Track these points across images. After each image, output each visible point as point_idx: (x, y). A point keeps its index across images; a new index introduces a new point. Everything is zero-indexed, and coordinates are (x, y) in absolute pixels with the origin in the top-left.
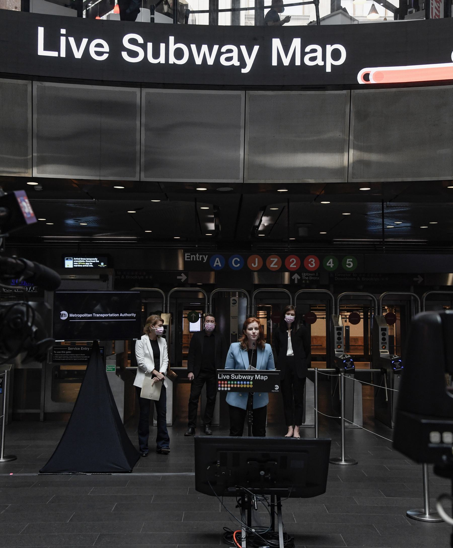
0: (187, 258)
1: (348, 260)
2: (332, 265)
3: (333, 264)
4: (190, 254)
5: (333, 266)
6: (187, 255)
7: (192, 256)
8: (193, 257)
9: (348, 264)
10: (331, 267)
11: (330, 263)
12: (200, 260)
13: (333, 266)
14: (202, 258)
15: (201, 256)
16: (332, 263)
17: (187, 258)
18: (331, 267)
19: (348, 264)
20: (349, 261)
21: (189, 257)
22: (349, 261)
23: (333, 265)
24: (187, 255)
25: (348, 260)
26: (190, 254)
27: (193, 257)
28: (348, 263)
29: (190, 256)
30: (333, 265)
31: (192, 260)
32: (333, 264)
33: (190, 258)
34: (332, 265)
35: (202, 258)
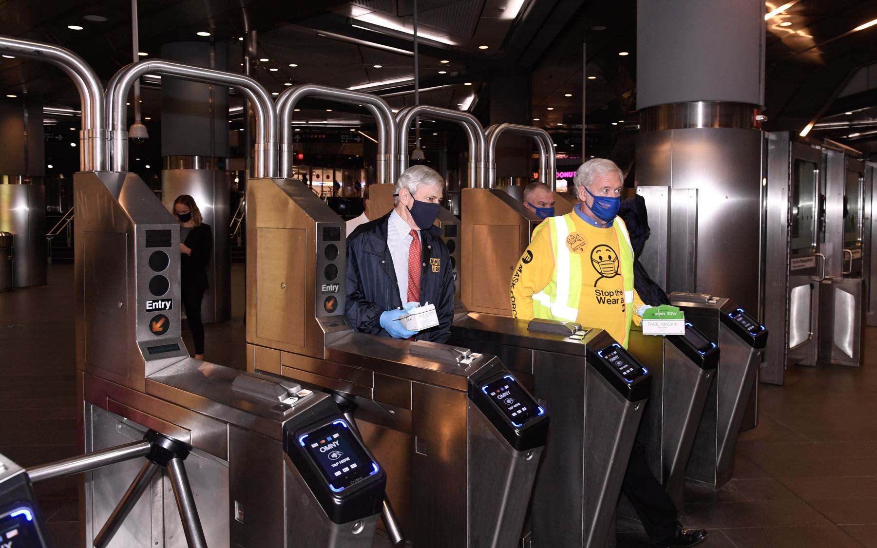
0: (149, 306)
4: (151, 302)
6: (149, 303)
7: (154, 304)
8: (156, 305)
12: (163, 307)
14: (165, 305)
15: (163, 303)
17: (149, 306)
21: (151, 305)
24: (149, 303)
26: (151, 302)
27: (156, 305)
29: (152, 303)
31: (154, 308)
33: (152, 306)
35: (165, 305)
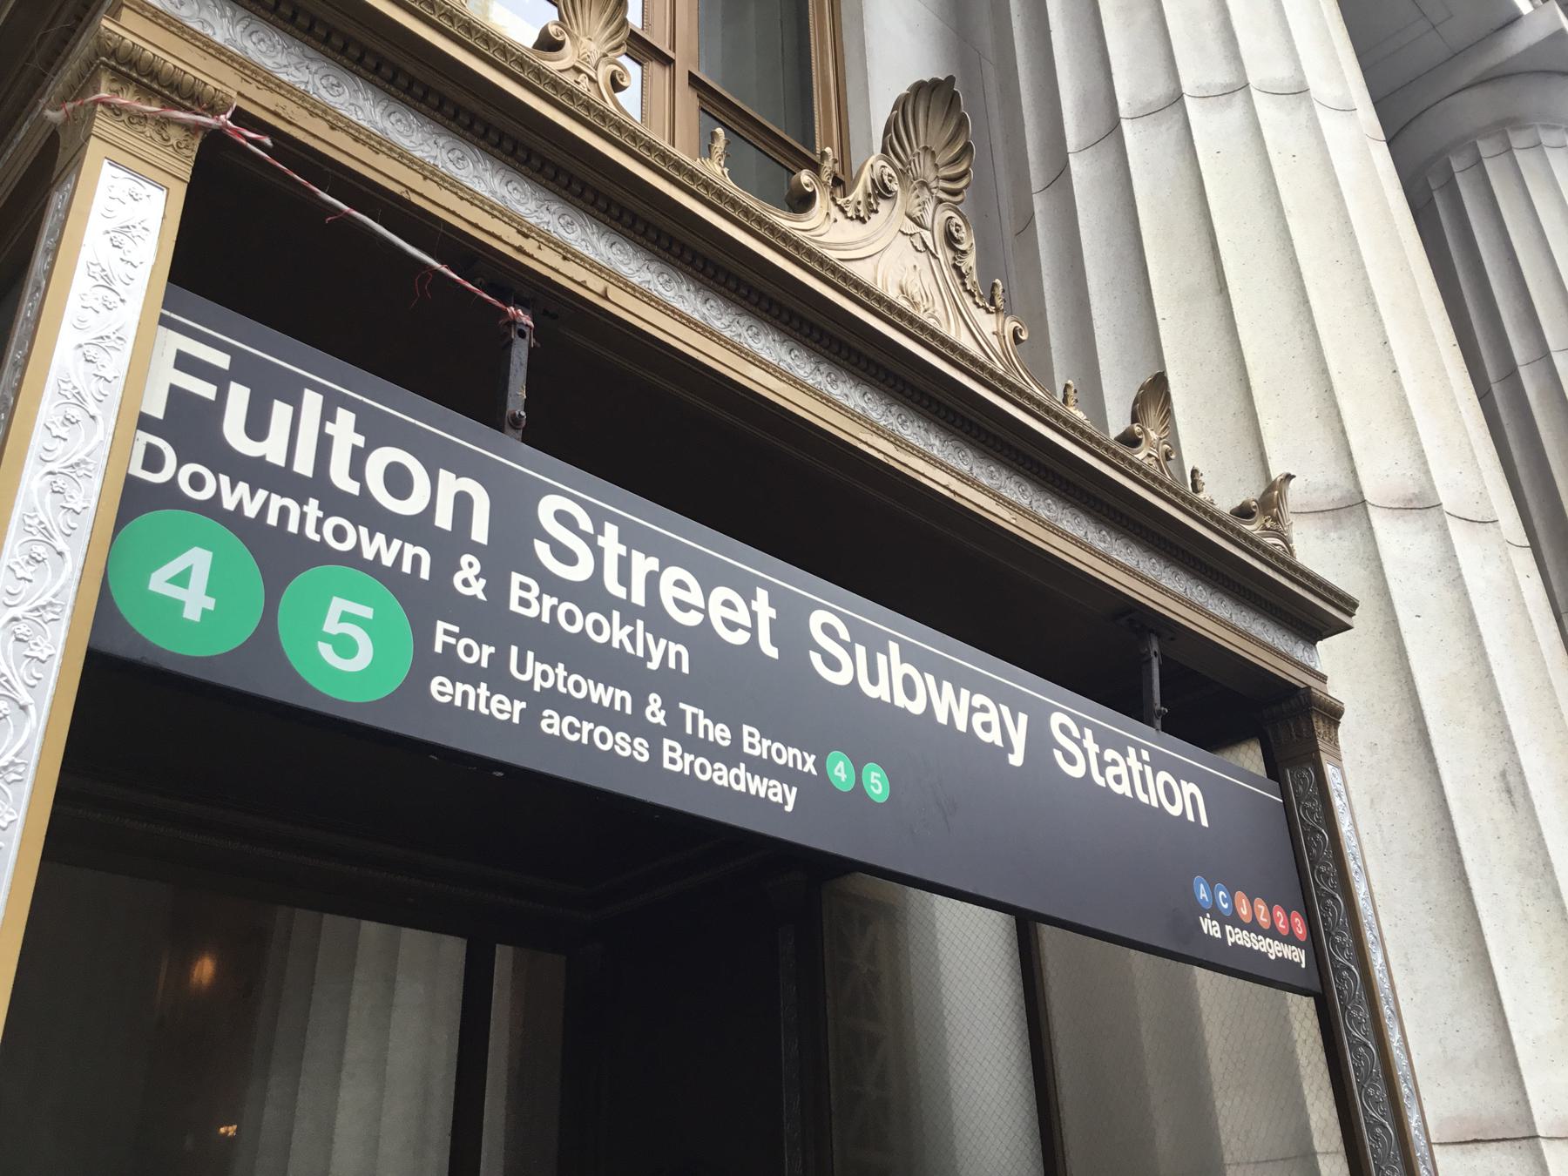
1: (338, 605)
2: (196, 602)
3: (208, 593)
5: (204, 611)
9: (328, 638)
10: (192, 613)
11: (182, 579)
13: (204, 611)
16: (200, 578)
18: (192, 613)
19: (328, 638)
20: (346, 617)
22: (346, 617)
23: (210, 604)
25: (338, 605)
28: (332, 626)
30: (210, 604)
32: (208, 593)
34: (196, 602)
